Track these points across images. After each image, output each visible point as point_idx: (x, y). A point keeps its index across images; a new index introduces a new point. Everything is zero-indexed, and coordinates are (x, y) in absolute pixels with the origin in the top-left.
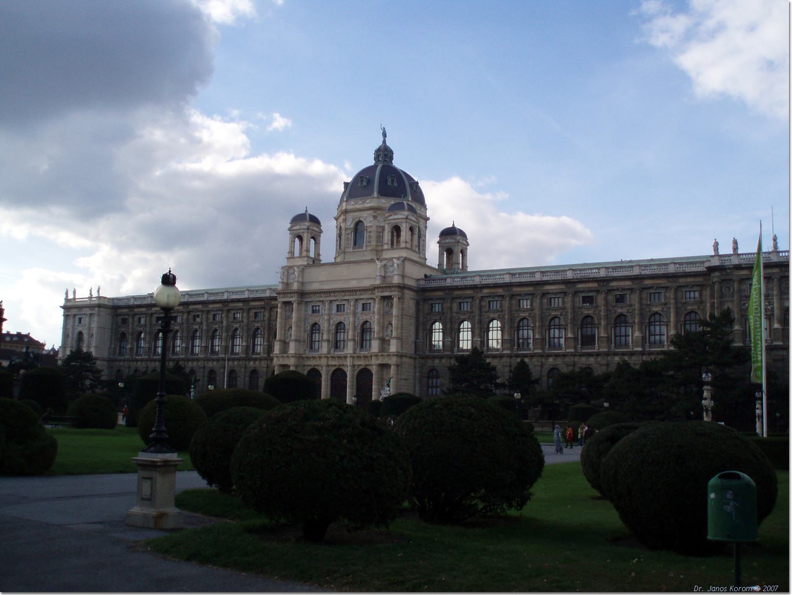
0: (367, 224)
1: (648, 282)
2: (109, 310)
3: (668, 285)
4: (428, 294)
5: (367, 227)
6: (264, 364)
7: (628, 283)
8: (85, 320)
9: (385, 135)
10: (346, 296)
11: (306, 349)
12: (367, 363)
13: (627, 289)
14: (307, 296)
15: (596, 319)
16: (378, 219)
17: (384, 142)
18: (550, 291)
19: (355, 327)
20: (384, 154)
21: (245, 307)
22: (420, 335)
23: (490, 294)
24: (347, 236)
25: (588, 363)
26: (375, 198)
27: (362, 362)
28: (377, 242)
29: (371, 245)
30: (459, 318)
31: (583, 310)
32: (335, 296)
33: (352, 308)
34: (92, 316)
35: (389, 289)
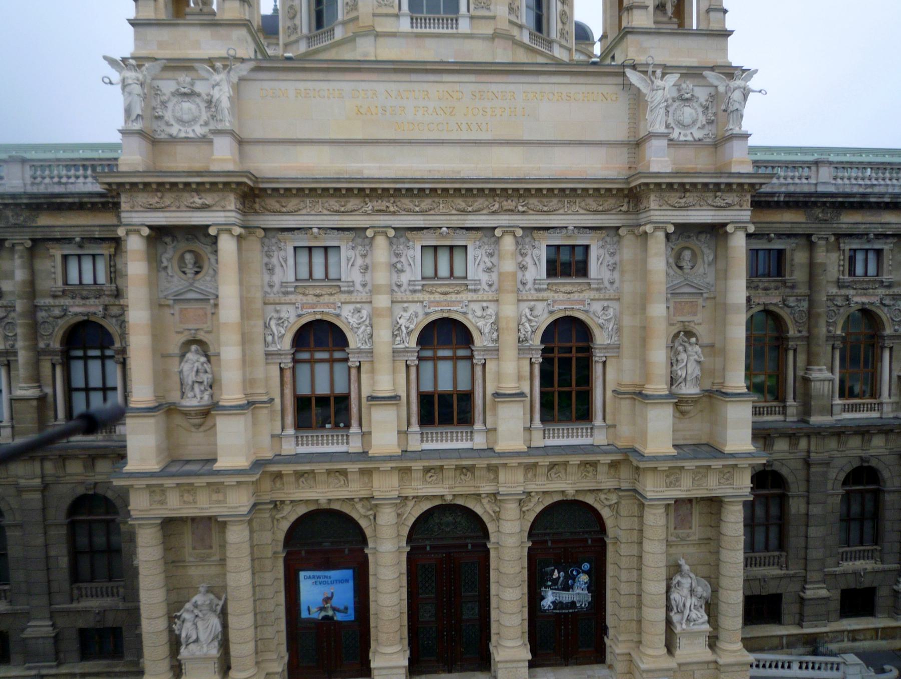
11: (279, 432)
14: (273, 203)
19: (519, 341)
29: (494, 18)
30: (847, 299)
32: (423, 213)
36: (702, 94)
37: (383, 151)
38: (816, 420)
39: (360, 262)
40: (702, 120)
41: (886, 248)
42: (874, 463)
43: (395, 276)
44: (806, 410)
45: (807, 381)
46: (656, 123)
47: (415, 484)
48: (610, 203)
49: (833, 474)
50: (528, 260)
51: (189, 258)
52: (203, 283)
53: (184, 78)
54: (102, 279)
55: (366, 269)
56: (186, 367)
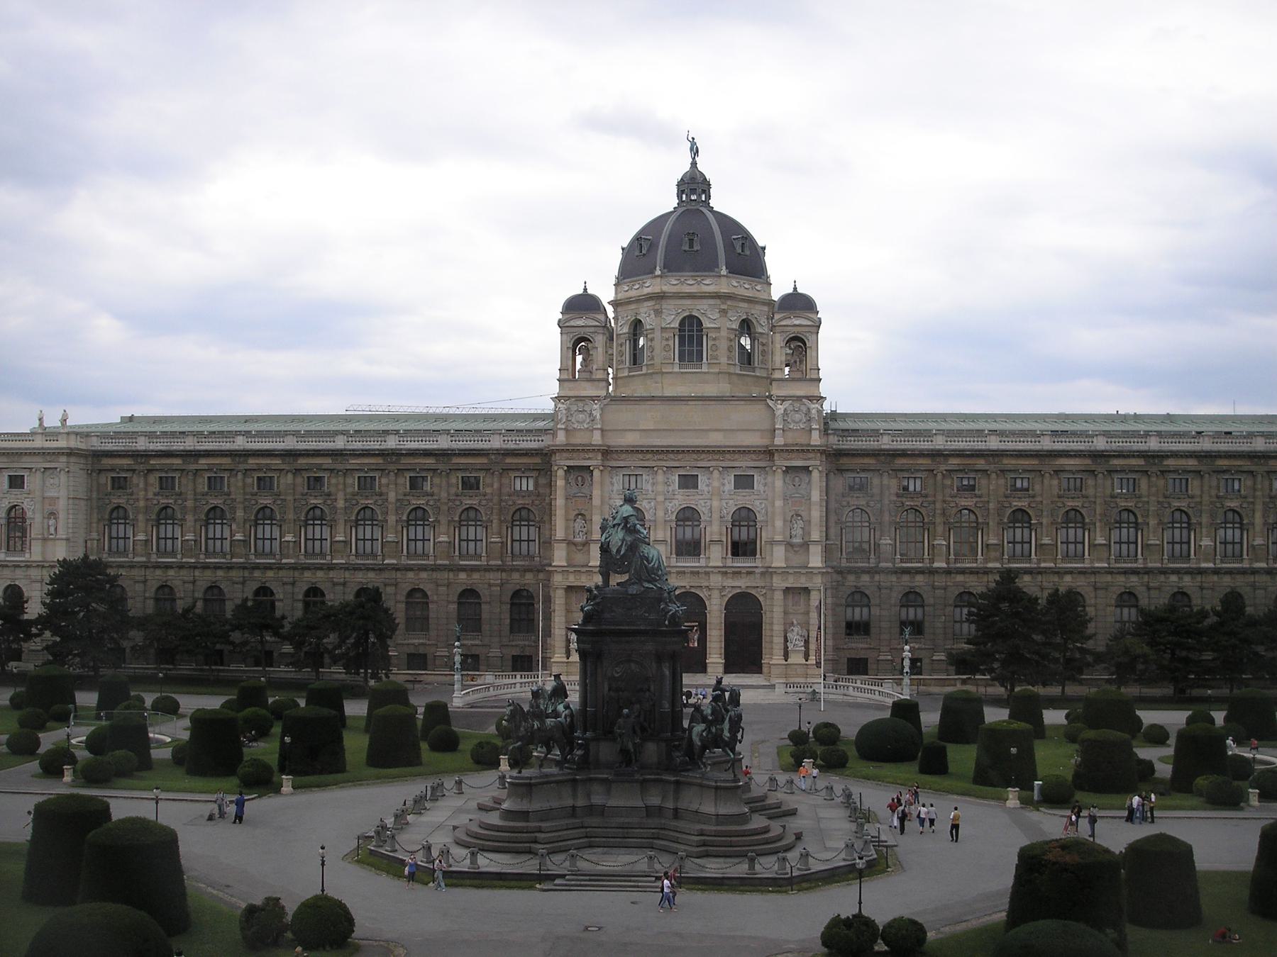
0: (706, 324)
2: (82, 461)
3: (1252, 468)
4: (844, 460)
6: (494, 577)
7: (1192, 463)
8: (32, 482)
9: (695, 151)
12: (749, 584)
13: (1190, 472)
14: (615, 456)
16: (730, 313)
17: (694, 164)
18: (1067, 468)
21: (440, 467)
22: (832, 531)
23: (961, 468)
24: (665, 343)
25: (1128, 585)
26: (724, 276)
27: (742, 583)
28: (729, 358)
31: (1118, 500)
32: (678, 460)
34: (48, 473)
35: (801, 455)
36: (804, 409)
39: (651, 481)
43: (666, 488)
48: (762, 456)
50: (726, 481)
51: (579, 478)
52: (585, 490)
53: (580, 404)
54: (531, 488)
56: (576, 525)
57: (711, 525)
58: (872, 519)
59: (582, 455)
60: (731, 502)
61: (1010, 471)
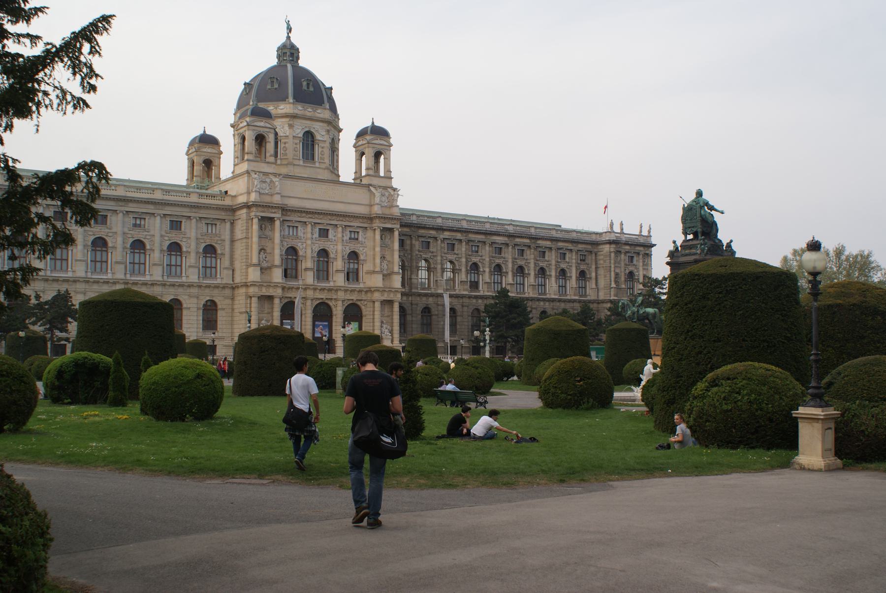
0: (318, 137)
1: (560, 244)
3: (572, 248)
5: (319, 140)
9: (290, 30)
10: (333, 220)
15: (526, 270)
17: (288, 38)
20: (288, 52)
24: (295, 146)
27: (354, 297)
32: (320, 219)
33: (340, 235)
36: (387, 194)
37: (311, 201)
38: (413, 290)
40: (387, 201)
41: (431, 241)
42: (429, 306)
44: (411, 288)
45: (411, 279)
46: (377, 200)
47: (317, 294)
48: (365, 220)
49: (418, 309)
51: (263, 226)
55: (304, 233)
57: (336, 261)
58: (406, 264)
59: (270, 210)
60: (347, 247)
61: (471, 241)
